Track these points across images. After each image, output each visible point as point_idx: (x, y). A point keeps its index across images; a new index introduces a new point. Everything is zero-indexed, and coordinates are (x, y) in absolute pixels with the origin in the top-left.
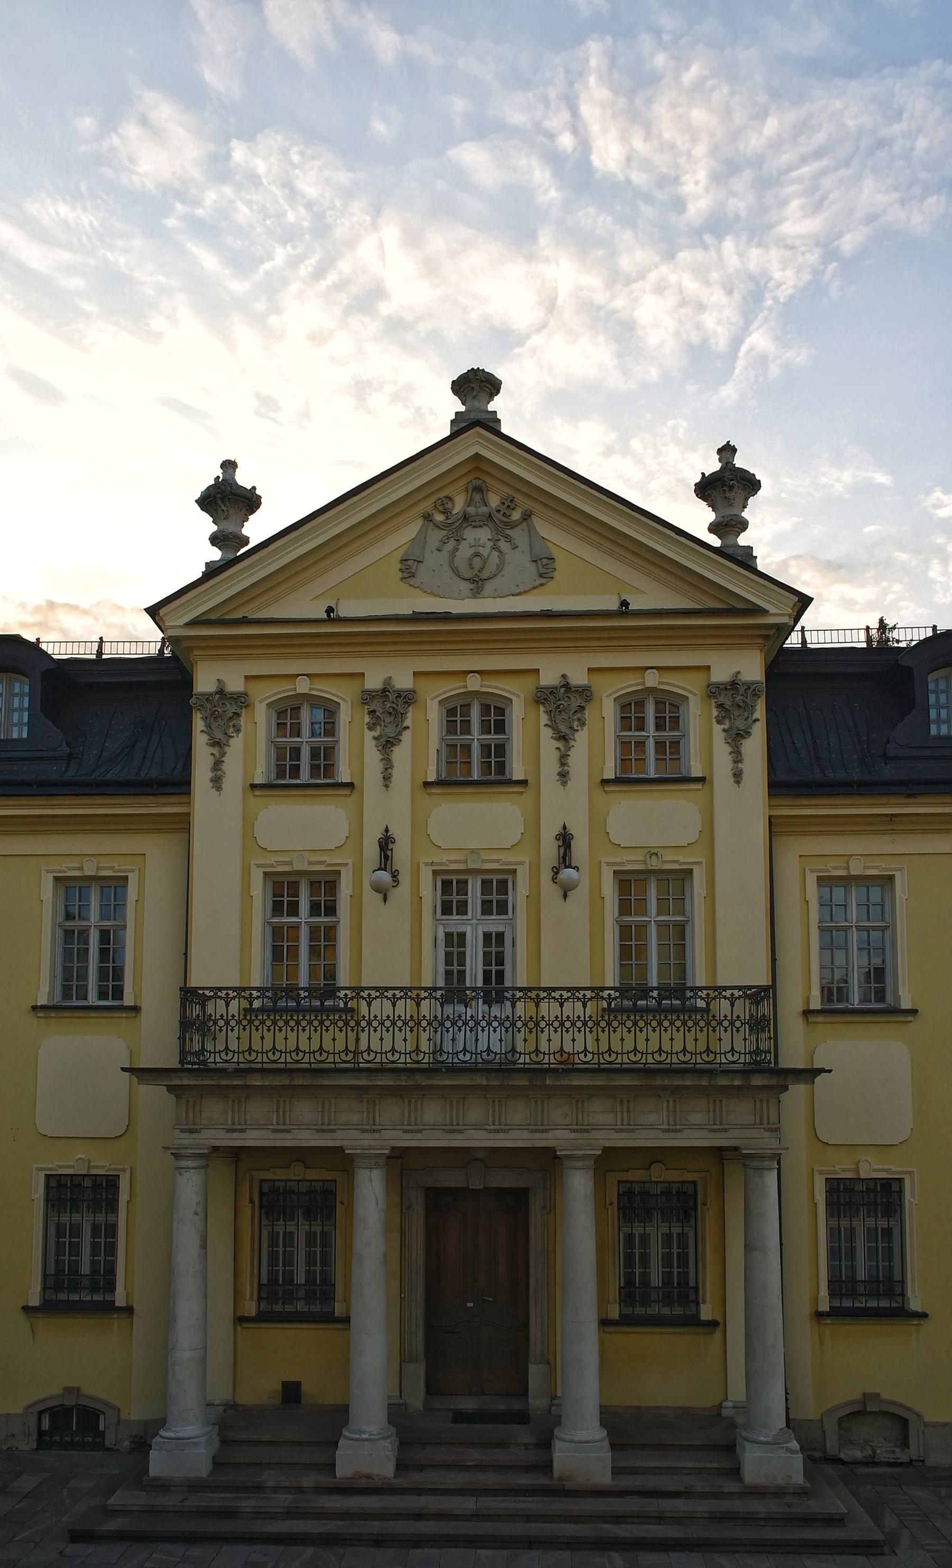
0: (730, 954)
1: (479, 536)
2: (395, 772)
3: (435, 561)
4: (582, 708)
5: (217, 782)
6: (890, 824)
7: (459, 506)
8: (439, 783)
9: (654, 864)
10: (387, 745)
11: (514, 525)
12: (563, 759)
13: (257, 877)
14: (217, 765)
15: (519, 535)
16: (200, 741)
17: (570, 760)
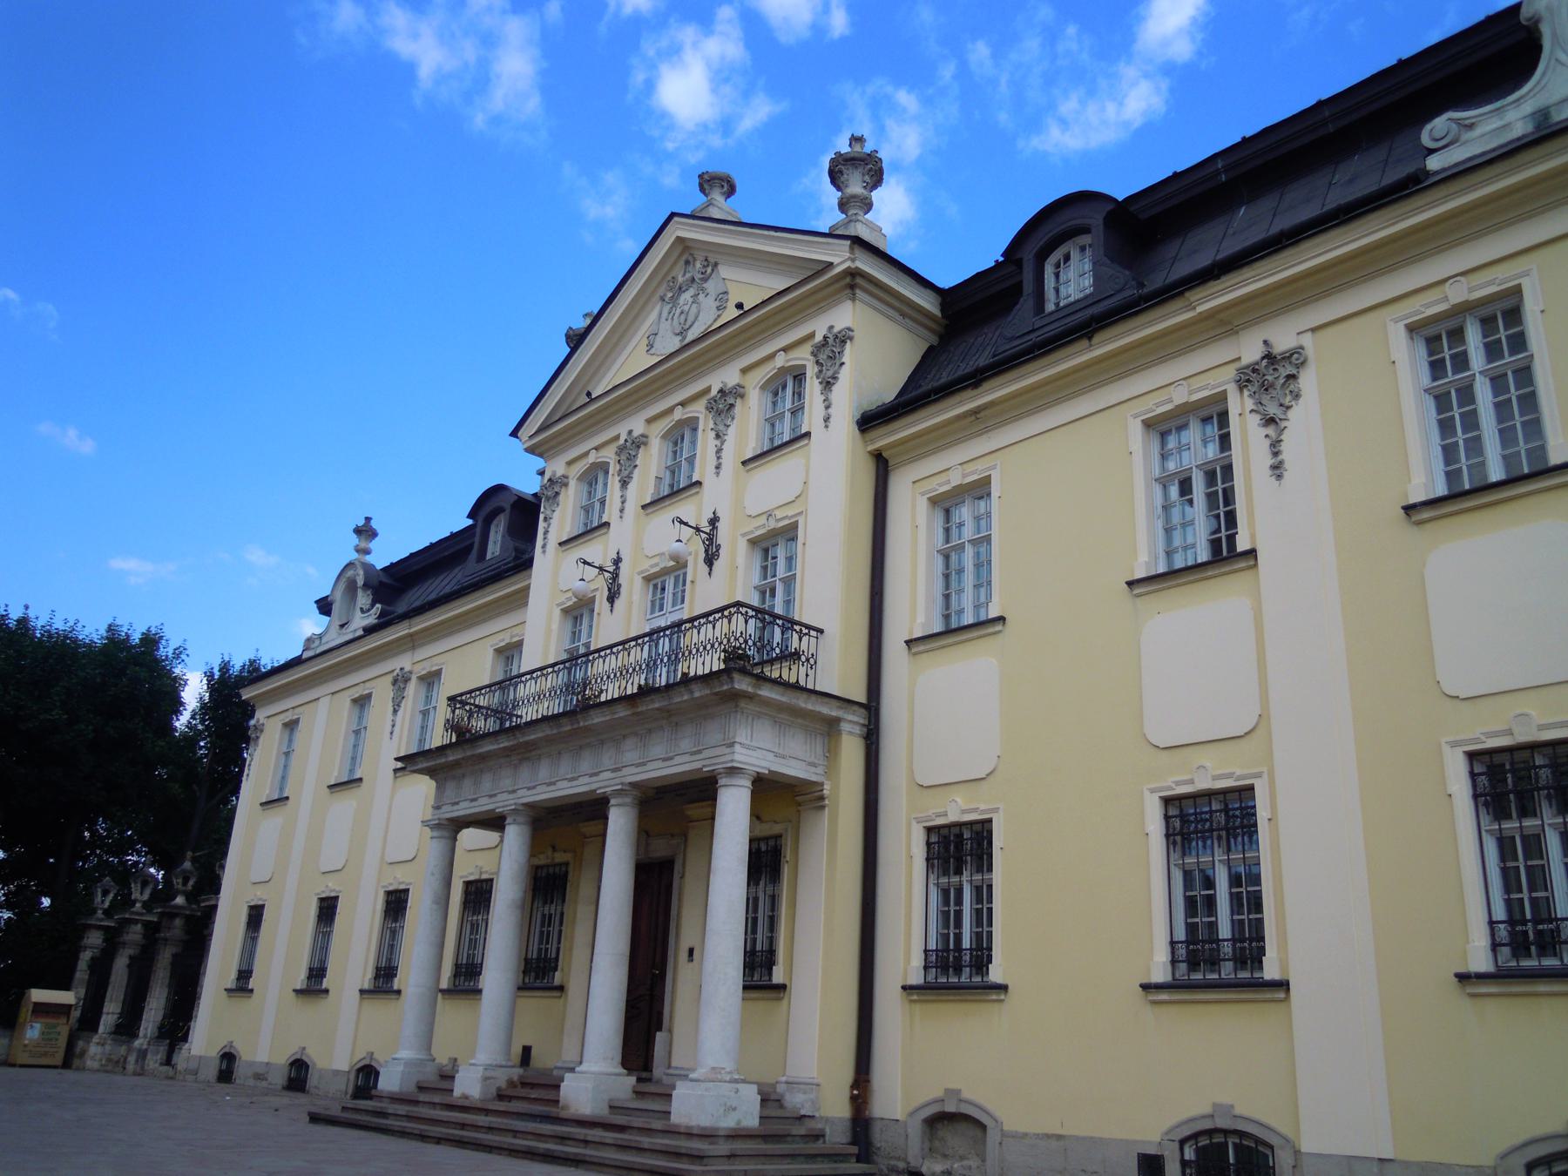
0: (825, 593)
1: (687, 296)
2: (627, 505)
3: (665, 326)
4: (732, 406)
5: (544, 546)
6: (980, 422)
7: (680, 279)
8: (652, 503)
9: (772, 524)
10: (624, 484)
11: (705, 280)
12: (719, 451)
13: (557, 612)
14: (546, 532)
15: (711, 286)
16: (542, 517)
17: (724, 454)
